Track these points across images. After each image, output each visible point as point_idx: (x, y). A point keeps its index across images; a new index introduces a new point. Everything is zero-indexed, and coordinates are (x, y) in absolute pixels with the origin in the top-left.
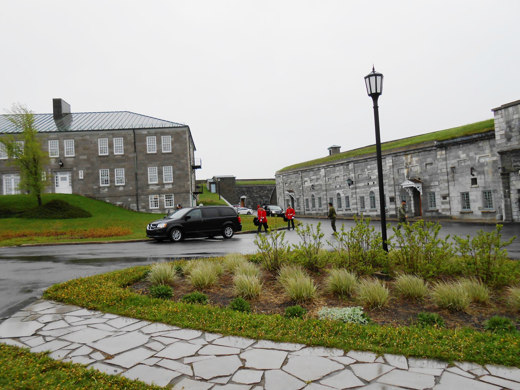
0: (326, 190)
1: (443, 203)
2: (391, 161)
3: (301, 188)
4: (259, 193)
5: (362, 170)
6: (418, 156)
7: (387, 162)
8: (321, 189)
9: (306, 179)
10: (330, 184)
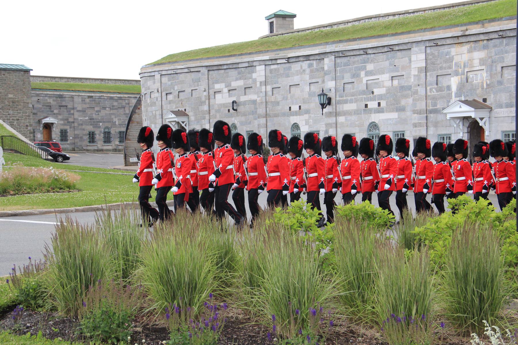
0: (266, 116)
2: (423, 56)
3: (206, 108)
4: (89, 112)
5: (356, 75)
6: (485, 47)
7: (414, 58)
8: (254, 113)
9: (217, 87)
10: (278, 103)
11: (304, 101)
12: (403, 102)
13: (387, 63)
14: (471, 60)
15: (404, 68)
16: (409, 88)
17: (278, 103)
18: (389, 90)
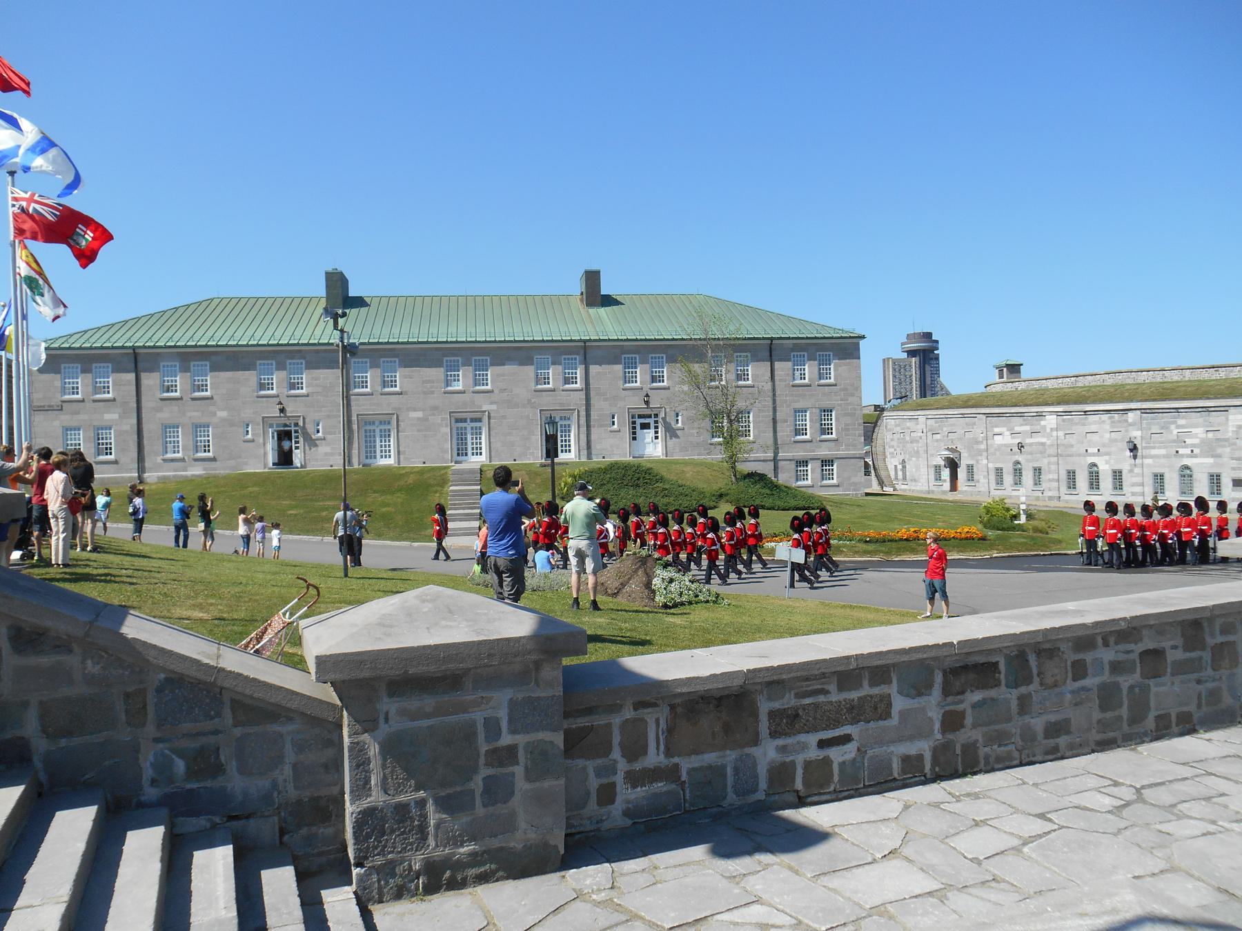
3: (983, 447)
5: (1165, 427)
7: (1231, 417)
9: (997, 430)
10: (1072, 446)
11: (1104, 445)
12: (1219, 451)
13: (1201, 420)
15: (1219, 425)
16: (1227, 440)
17: (1072, 446)
18: (1203, 441)
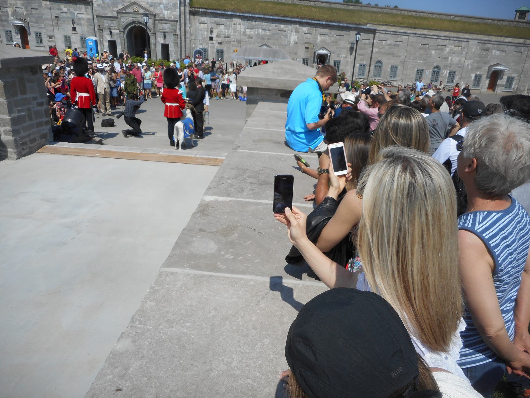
1: (49, 41)
14: (17, 3)
